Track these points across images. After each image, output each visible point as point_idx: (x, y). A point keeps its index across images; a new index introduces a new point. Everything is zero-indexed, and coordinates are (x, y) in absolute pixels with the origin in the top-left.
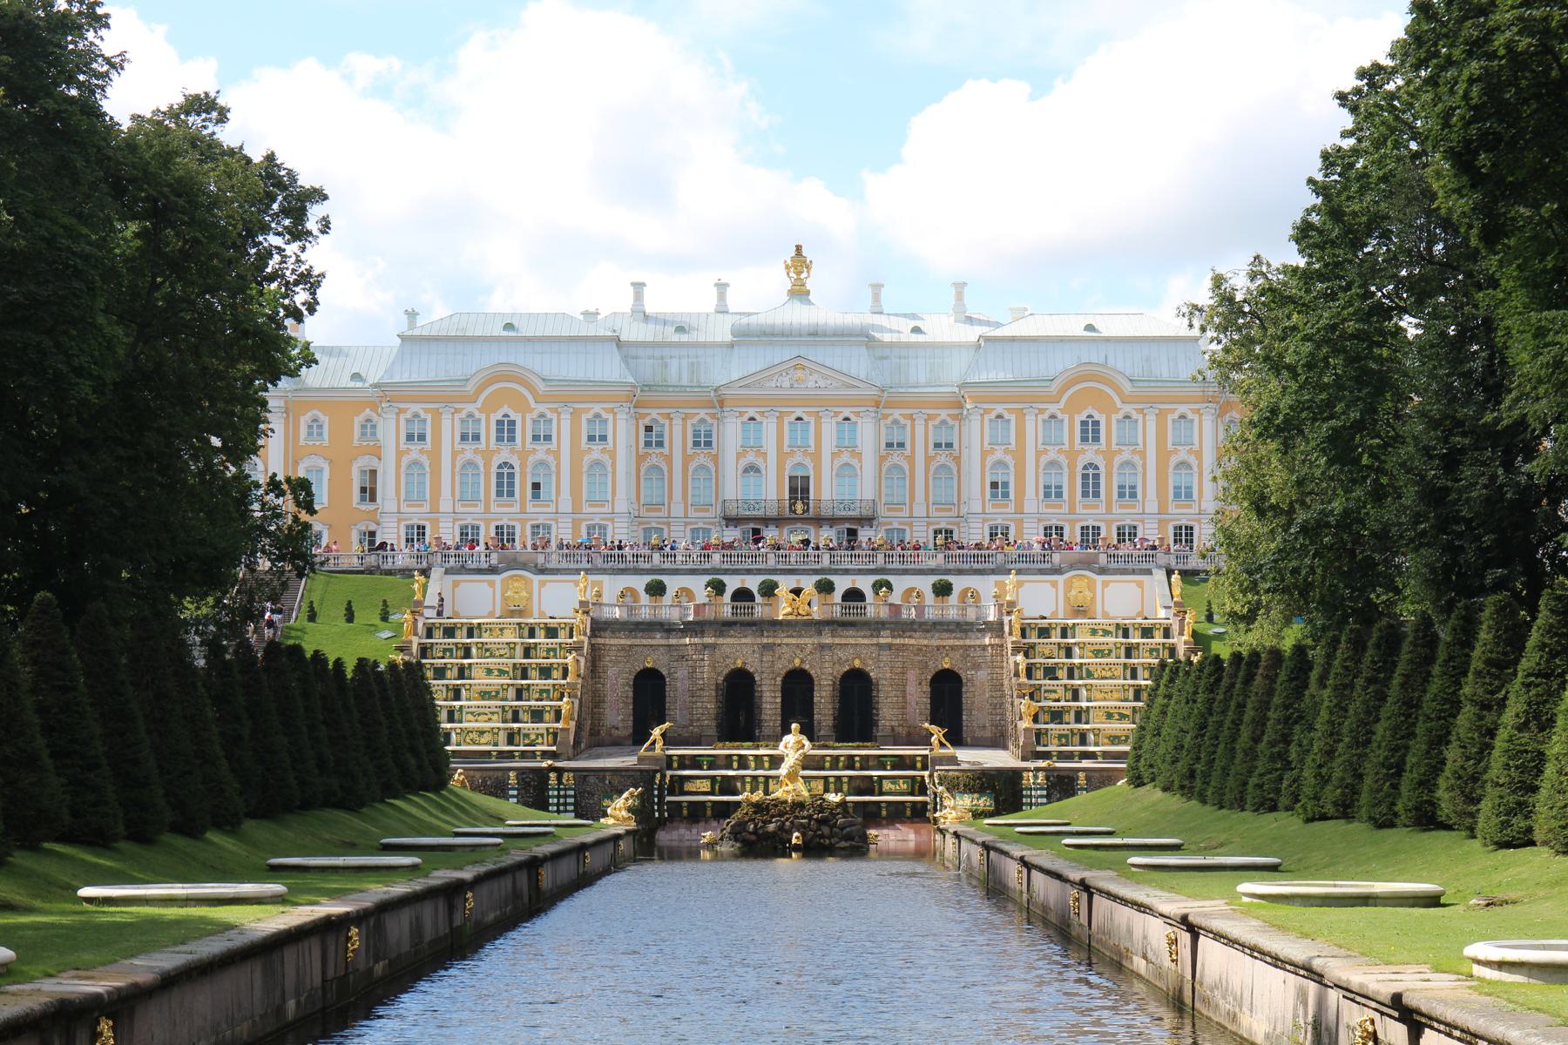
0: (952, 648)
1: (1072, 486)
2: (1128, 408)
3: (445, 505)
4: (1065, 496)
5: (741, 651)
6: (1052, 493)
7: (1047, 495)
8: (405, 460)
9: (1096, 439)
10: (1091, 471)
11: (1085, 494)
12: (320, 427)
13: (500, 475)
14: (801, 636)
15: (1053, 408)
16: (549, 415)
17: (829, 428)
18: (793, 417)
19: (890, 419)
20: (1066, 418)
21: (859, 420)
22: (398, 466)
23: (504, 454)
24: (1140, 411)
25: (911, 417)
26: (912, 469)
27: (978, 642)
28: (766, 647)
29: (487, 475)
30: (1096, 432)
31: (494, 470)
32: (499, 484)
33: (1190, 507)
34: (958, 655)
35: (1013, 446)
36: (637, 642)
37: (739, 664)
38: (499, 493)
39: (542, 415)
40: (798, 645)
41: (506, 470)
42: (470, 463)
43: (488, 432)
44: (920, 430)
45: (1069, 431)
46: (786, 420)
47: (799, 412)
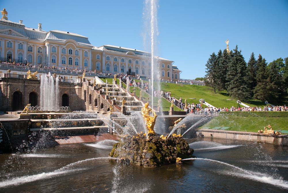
0: (67, 89)
1: (67, 61)
2: (77, 49)
4: (66, 63)
5: (19, 87)
6: (63, 62)
7: (63, 63)
9: (72, 54)
10: (71, 60)
11: (69, 64)
14: (35, 84)
15: (64, 47)
17: (17, 45)
18: (8, 42)
19: (29, 45)
20: (66, 49)
21: (24, 44)
24: (80, 50)
25: (34, 45)
26: (34, 56)
27: (74, 88)
28: (25, 86)
30: (72, 52)
33: (87, 68)
34: (68, 90)
35: (56, 53)
37: (18, 90)
40: (34, 86)
44: (35, 48)
45: (67, 52)
46: (7, 42)
47: (10, 40)
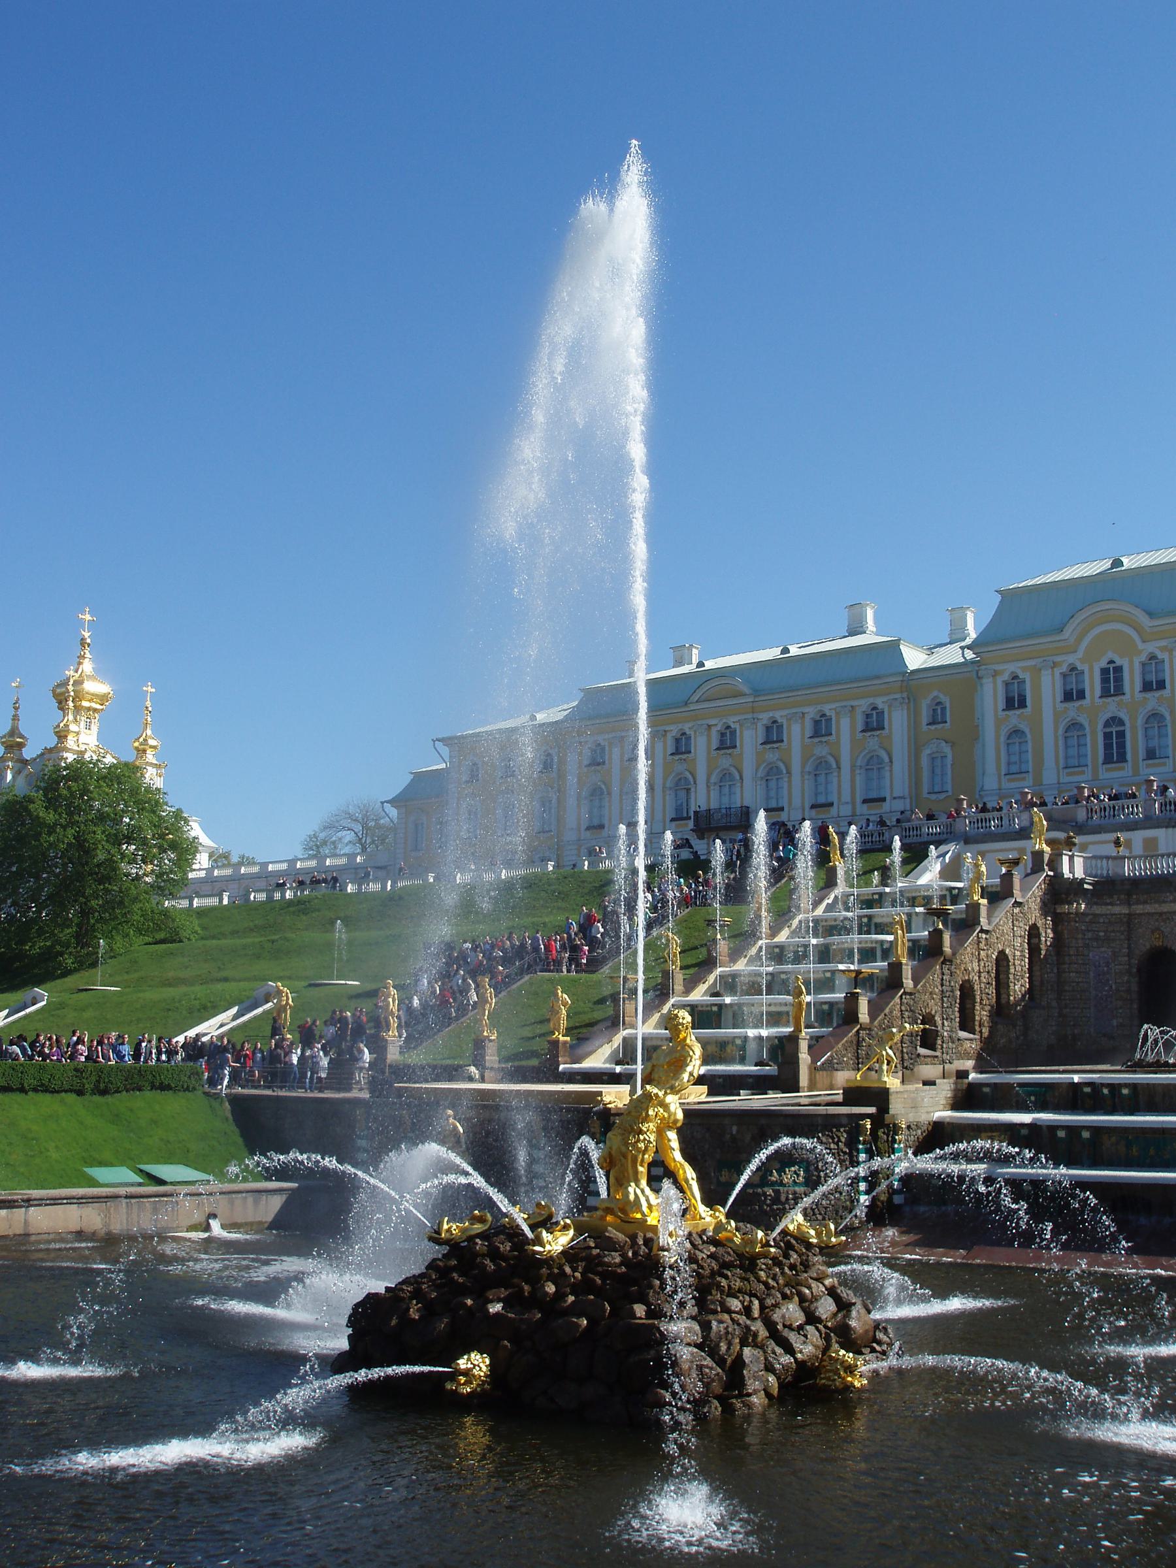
3: (1050, 776)
8: (1004, 733)
12: (944, 709)
13: (1108, 736)
16: (1160, 655)
22: (997, 737)
23: (1111, 707)
29: (1094, 732)
31: (1100, 726)
32: (1108, 746)
36: (1139, 909)
38: (1108, 759)
39: (1153, 657)
41: (1114, 729)
42: (1074, 726)
43: (1093, 685)
